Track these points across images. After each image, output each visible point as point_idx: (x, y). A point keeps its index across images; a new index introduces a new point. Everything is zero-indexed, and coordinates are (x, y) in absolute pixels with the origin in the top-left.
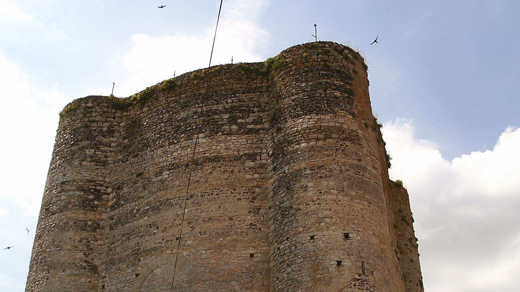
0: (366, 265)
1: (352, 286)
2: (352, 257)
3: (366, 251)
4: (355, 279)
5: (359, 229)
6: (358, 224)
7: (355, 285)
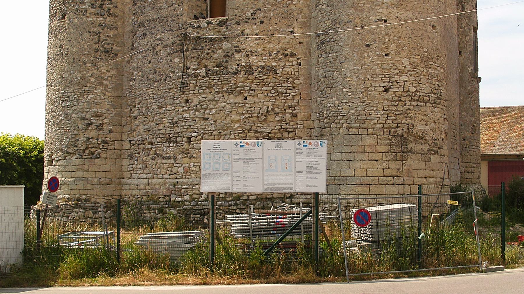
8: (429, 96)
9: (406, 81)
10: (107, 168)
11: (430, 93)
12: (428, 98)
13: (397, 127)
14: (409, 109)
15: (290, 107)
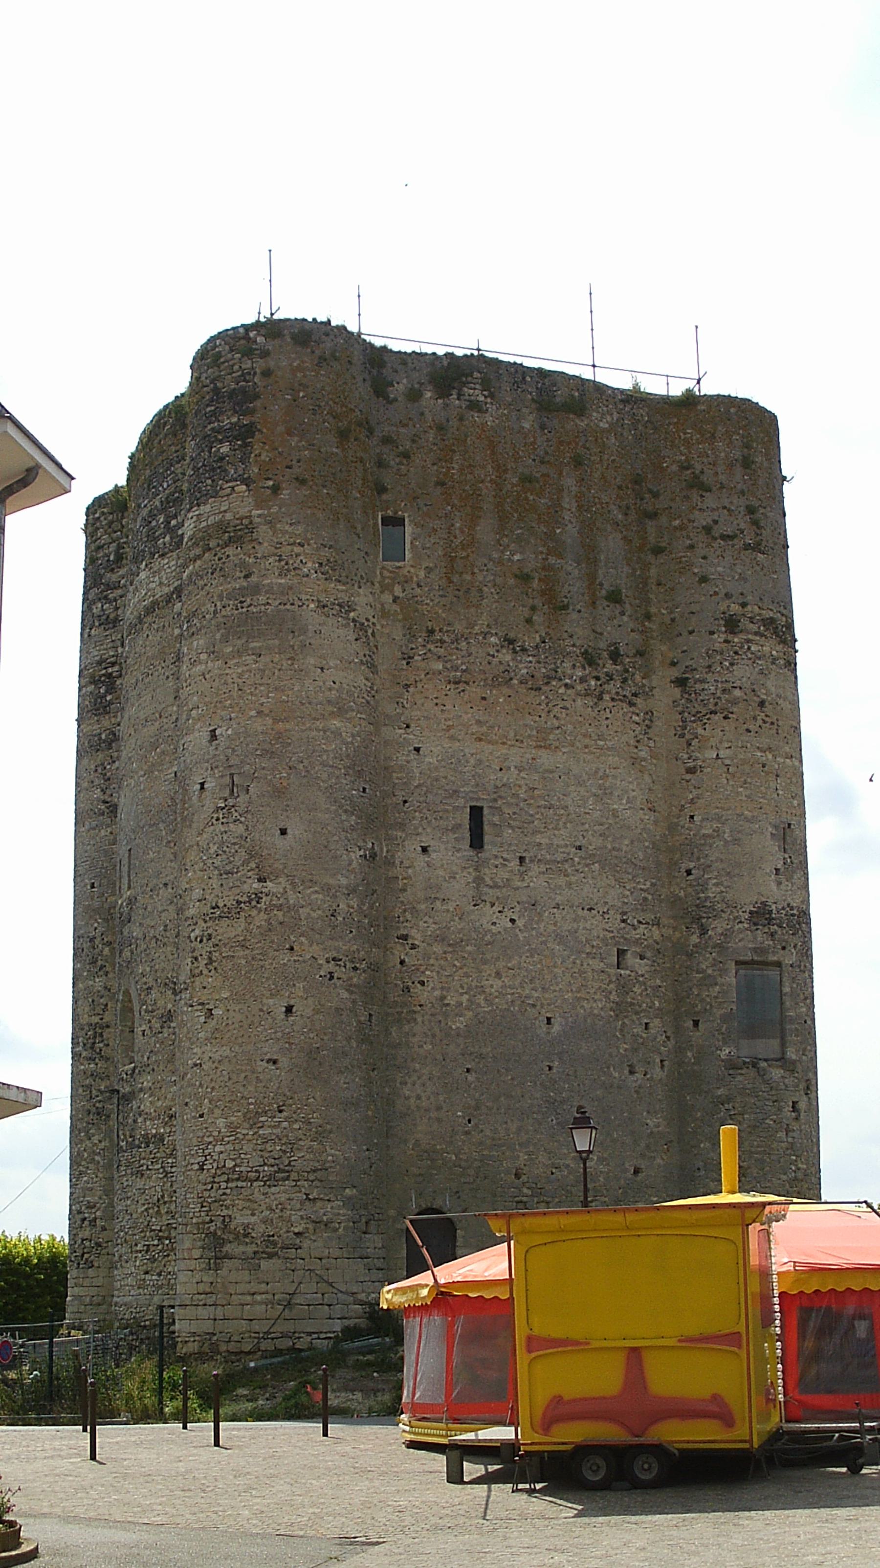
1: (215, 822)
3: (239, 753)
4: (218, 809)
5: (233, 715)
6: (231, 706)
8: (256, 1171)
9: (222, 1152)
11: (260, 1166)
12: (254, 1174)
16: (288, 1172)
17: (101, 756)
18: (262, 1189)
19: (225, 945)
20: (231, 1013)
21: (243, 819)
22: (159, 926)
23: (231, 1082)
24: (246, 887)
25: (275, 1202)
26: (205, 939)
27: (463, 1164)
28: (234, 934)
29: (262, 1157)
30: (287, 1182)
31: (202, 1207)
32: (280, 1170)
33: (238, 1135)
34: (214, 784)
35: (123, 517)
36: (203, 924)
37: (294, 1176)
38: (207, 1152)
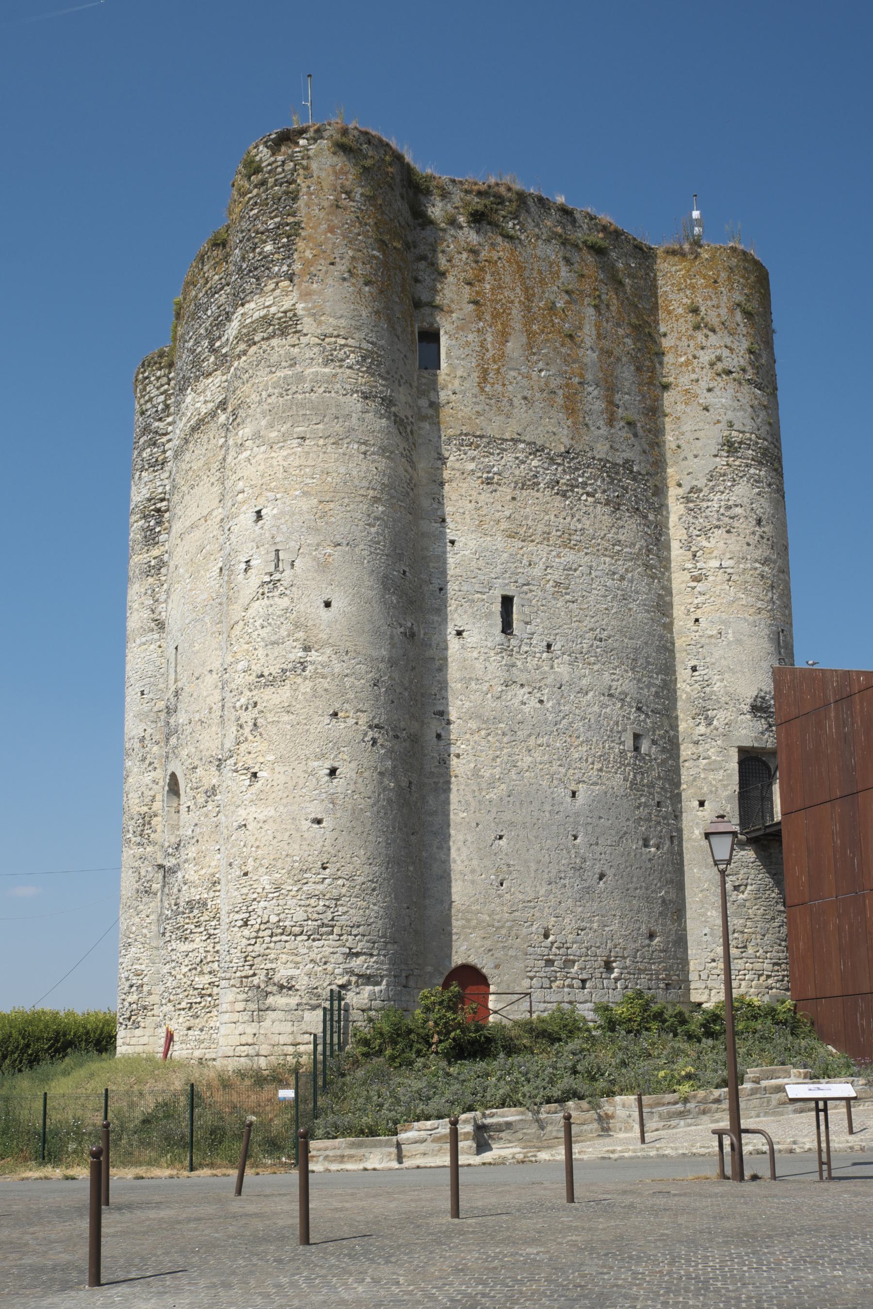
0: (282, 555)
2: (262, 548)
5: (278, 496)
7: (263, 594)
8: (301, 926)
10: (144, 1040)
12: (298, 929)
13: (254, 975)
14: (268, 948)
15: (217, 952)
16: (333, 926)
17: (150, 580)
18: (306, 943)
19: (270, 711)
20: (276, 776)
21: (288, 592)
22: (205, 709)
23: (276, 840)
24: (292, 657)
25: (319, 956)
26: (250, 707)
27: (496, 924)
28: (279, 700)
29: (306, 912)
30: (331, 937)
31: (246, 961)
32: (323, 925)
33: (283, 891)
34: (259, 561)
35: (170, 373)
36: (249, 693)
37: (337, 930)
38: (250, 909)
